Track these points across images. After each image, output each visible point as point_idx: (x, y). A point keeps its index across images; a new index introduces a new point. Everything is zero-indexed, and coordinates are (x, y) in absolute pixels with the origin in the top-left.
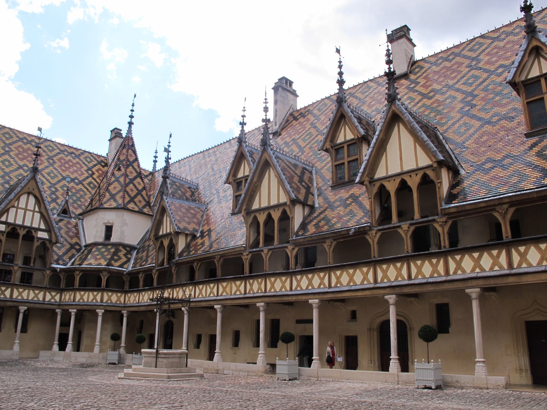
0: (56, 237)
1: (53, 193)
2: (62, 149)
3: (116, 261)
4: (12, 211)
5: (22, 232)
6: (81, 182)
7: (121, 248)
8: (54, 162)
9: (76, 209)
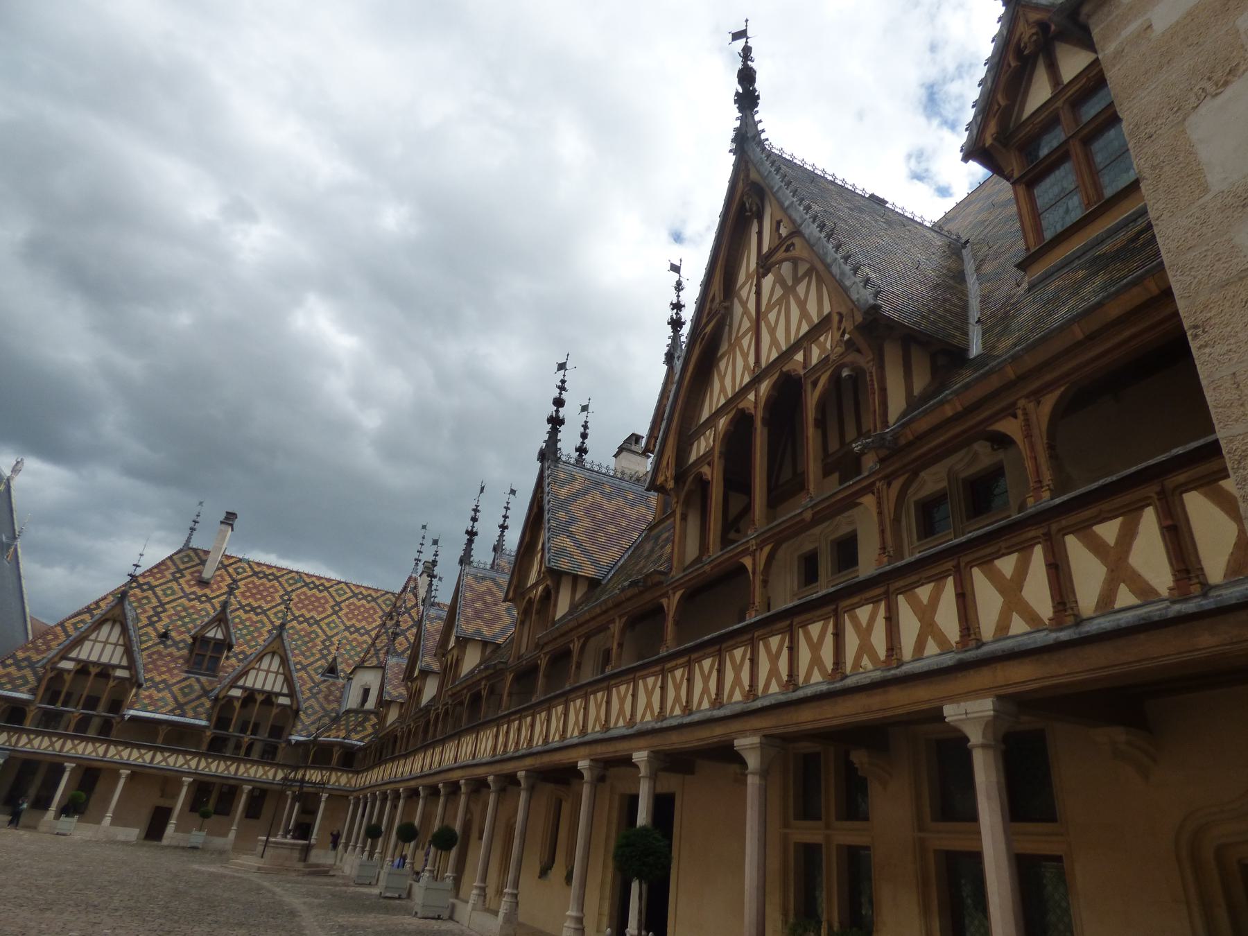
0: (298, 702)
1: (326, 648)
2: (357, 591)
3: (357, 733)
4: (252, 673)
5: (260, 698)
6: (368, 632)
7: (372, 717)
8: (341, 609)
9: (349, 666)
